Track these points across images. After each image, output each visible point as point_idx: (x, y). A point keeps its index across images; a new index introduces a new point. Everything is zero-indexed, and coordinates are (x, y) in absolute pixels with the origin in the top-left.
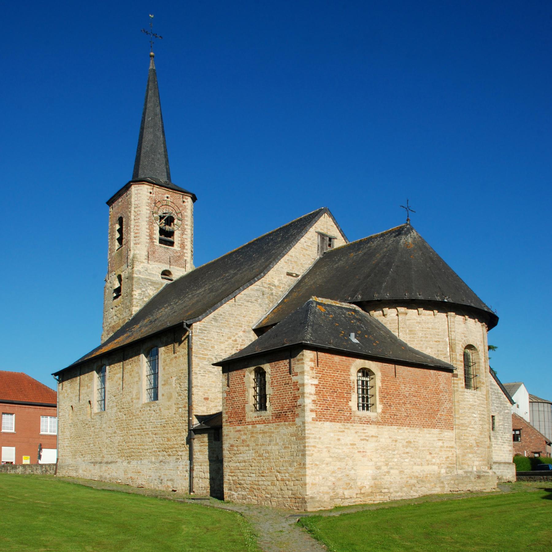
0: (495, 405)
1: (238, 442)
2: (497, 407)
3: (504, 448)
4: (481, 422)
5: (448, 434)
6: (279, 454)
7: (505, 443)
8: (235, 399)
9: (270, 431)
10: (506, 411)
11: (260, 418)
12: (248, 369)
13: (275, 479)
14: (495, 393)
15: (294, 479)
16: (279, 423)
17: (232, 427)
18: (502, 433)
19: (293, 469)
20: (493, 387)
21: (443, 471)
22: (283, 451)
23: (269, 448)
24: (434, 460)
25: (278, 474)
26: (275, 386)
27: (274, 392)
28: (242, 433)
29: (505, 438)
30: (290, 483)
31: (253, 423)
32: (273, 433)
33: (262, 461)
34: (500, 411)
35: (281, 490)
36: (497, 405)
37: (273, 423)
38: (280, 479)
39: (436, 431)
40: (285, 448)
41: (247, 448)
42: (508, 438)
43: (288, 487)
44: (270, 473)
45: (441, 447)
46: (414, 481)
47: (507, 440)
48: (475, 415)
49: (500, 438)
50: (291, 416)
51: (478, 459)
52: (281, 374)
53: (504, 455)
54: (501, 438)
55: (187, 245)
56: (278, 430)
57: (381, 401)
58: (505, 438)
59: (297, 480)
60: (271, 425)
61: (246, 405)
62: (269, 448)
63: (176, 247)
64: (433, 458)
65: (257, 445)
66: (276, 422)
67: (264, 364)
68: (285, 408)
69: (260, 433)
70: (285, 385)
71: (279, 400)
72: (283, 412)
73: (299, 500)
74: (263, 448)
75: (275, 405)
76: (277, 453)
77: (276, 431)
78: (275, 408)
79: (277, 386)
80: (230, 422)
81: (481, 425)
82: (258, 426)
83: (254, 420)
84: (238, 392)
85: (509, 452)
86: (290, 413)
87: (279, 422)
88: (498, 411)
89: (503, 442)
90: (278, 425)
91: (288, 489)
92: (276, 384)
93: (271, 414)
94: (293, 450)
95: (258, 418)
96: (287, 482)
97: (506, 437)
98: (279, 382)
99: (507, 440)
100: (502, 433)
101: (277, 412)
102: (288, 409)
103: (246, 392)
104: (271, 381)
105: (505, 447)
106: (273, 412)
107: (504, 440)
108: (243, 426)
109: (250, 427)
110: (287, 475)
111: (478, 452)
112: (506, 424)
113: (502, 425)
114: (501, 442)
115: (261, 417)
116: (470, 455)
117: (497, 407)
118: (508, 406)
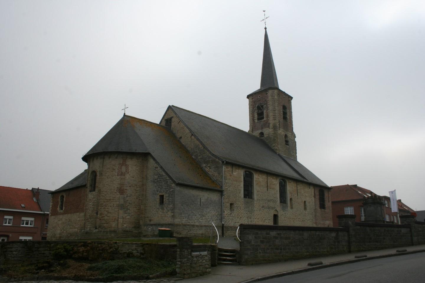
0: (164, 188)
2: (165, 189)
3: (168, 214)
4: (93, 207)
5: (82, 214)
7: (169, 211)
10: (171, 190)
14: (164, 180)
18: (167, 205)
20: (163, 177)
21: (79, 231)
24: (76, 226)
29: (169, 208)
34: (167, 191)
36: (165, 188)
39: (78, 214)
42: (171, 207)
45: (79, 220)
46: (69, 235)
47: (170, 209)
48: (90, 204)
49: (165, 209)
51: (89, 225)
53: (168, 219)
54: (166, 208)
55: (269, 115)
57: (65, 206)
58: (169, 208)
63: (265, 119)
64: (76, 225)
81: (93, 208)
85: (171, 217)
88: (165, 192)
89: (167, 211)
97: (170, 207)
99: (170, 209)
100: (167, 205)
105: (169, 214)
107: (168, 209)
111: (90, 221)
112: (170, 199)
113: (168, 200)
114: (166, 211)
116: (87, 223)
117: (165, 189)
118: (173, 186)
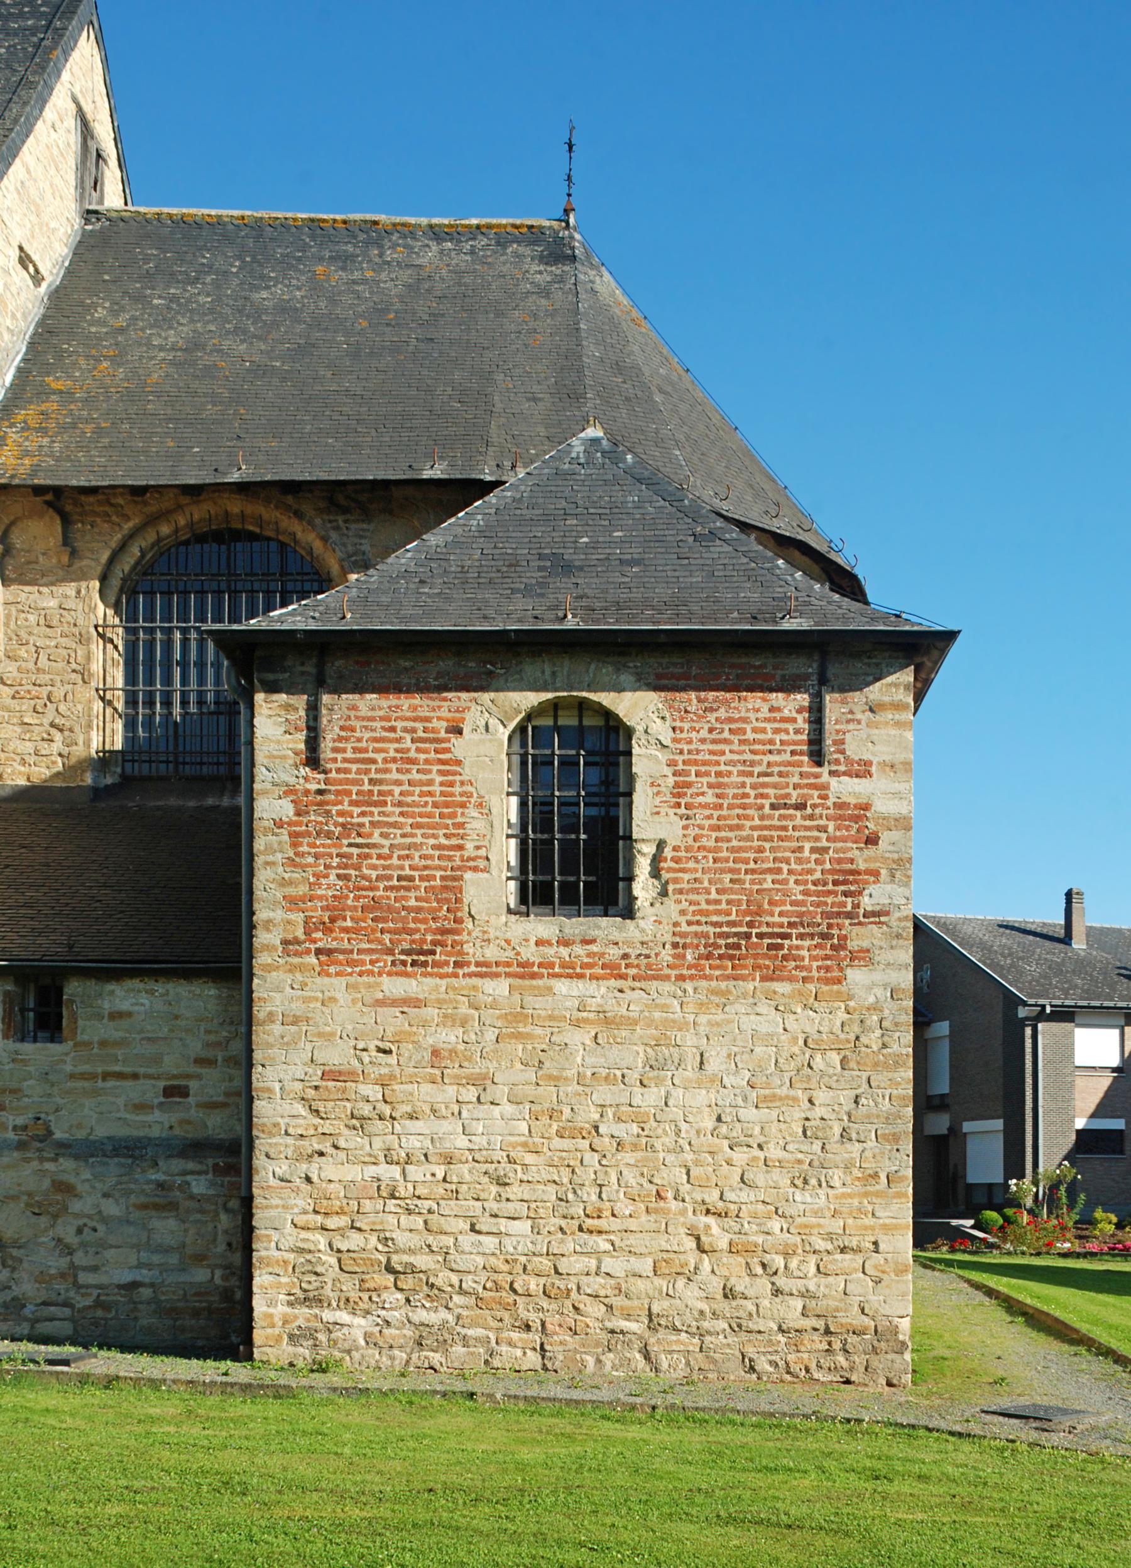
1: (392, 1060)
6: (724, 1129)
8: (376, 839)
9: (657, 1015)
11: (579, 950)
12: (486, 697)
13: (691, 1244)
15: (821, 1244)
16: (723, 985)
17: (342, 981)
19: (823, 1199)
22: (749, 1113)
23: (649, 1099)
25: (711, 1220)
26: (705, 806)
27: (692, 832)
28: (432, 1012)
30: (794, 1263)
31: (525, 971)
32: (682, 1027)
33: (592, 1159)
35: (729, 1294)
37: (681, 978)
38: (723, 1244)
40: (768, 1100)
41: (470, 1094)
43: (781, 1281)
44: (644, 1218)
50: (813, 958)
52: (748, 757)
56: (720, 1017)
59: (843, 1250)
60: (667, 987)
61: (468, 875)
62: (649, 1099)
65: (556, 1080)
66: (706, 977)
67: (620, 689)
68: (776, 919)
69: (577, 1024)
70: (773, 807)
71: (727, 877)
72: (760, 936)
73: (852, 1339)
74: (604, 1094)
75: (702, 898)
76: (709, 1123)
77: (703, 1019)
78: (701, 912)
79: (721, 806)
80: (319, 952)
82: (562, 987)
83: (529, 953)
84: (400, 804)
86: (807, 943)
87: (728, 978)
90: (715, 992)
91: (777, 1292)
92: (710, 798)
93: (668, 938)
94: (819, 1112)
95: (564, 952)
96: (779, 1261)
98: (731, 792)
101: (711, 930)
102: (791, 925)
103: (473, 812)
104: (671, 780)
106: (685, 928)
108: (443, 983)
109: (498, 988)
110: (775, 1225)
115: (594, 948)
